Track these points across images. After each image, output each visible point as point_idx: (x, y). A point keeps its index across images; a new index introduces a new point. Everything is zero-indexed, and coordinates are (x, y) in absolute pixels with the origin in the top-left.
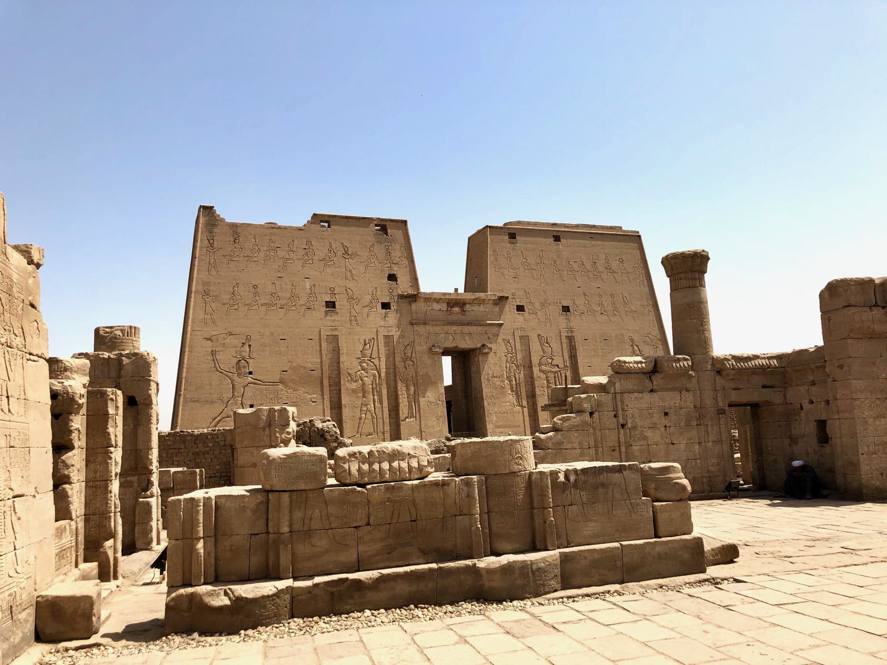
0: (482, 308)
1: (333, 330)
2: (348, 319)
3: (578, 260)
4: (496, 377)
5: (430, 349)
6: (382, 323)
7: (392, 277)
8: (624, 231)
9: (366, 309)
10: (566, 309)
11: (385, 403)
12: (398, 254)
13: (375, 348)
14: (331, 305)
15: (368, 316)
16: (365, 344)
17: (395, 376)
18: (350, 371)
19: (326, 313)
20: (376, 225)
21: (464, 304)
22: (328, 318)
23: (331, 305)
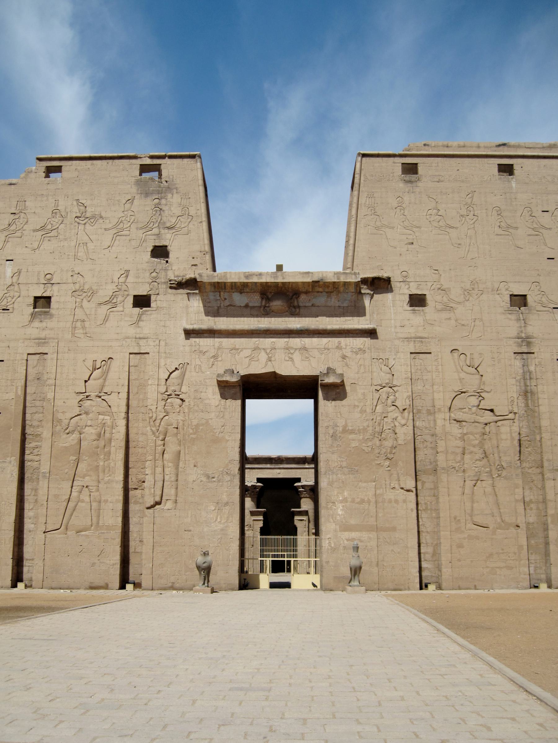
0: (334, 301)
1: (39, 344)
2: (69, 325)
4: (352, 432)
6: (132, 331)
7: (160, 252)
10: (519, 301)
12: (178, 212)
14: (42, 302)
15: (106, 319)
16: (95, 369)
18: (60, 416)
19: (33, 316)
20: (144, 169)
22: (36, 324)
23: (42, 302)
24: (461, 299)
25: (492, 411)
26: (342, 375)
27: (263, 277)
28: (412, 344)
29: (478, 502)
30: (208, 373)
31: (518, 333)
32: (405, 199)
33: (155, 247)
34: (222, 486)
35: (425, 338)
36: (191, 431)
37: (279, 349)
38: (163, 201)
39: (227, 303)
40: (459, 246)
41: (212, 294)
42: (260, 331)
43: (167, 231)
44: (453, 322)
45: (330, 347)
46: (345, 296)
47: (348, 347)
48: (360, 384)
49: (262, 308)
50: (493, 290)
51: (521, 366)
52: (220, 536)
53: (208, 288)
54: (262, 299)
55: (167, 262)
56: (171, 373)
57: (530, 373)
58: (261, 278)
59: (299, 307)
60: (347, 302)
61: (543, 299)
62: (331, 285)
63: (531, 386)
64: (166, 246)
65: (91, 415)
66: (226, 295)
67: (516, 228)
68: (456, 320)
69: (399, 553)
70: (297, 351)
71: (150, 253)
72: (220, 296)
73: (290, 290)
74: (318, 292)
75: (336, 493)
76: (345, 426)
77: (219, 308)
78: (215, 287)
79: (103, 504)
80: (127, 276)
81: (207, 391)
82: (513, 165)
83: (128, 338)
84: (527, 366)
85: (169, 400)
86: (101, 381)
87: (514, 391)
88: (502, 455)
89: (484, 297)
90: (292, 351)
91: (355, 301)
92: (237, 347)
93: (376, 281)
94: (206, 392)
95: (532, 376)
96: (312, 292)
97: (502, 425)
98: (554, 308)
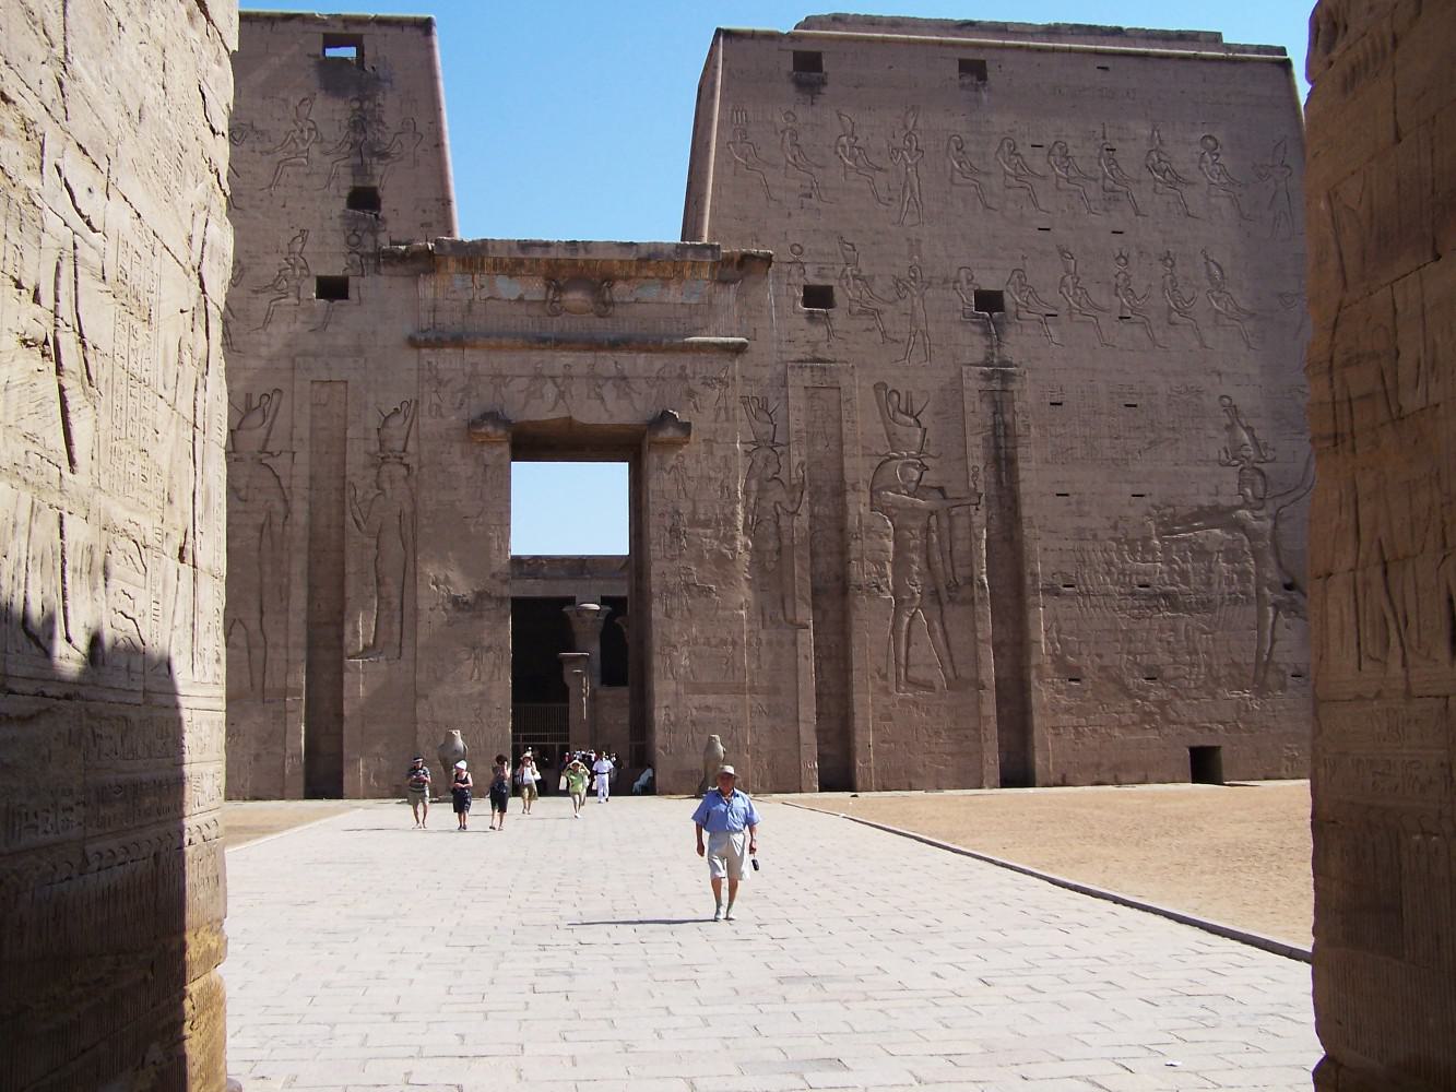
0: (673, 294)
3: (1048, 141)
4: (706, 524)
5: (473, 424)
7: (364, 199)
8: (1229, 47)
9: (263, 301)
10: (989, 301)
11: (299, 598)
13: (282, 422)
17: (344, 513)
20: (332, 41)
21: (610, 279)
24: (891, 295)
25: (941, 490)
27: (551, 249)
28: (807, 373)
29: (916, 644)
30: (453, 418)
31: (987, 358)
33: (355, 187)
34: (481, 617)
35: (829, 362)
36: (425, 522)
37: (577, 377)
38: (366, 104)
39: (485, 293)
40: (890, 202)
41: (458, 276)
43: (375, 159)
44: (877, 336)
45: (666, 375)
46: (695, 285)
47: (697, 377)
48: (720, 440)
49: (548, 304)
50: (946, 281)
51: (991, 414)
52: (477, 705)
53: (452, 265)
54: (548, 287)
55: (376, 216)
56: (386, 418)
57: (1006, 427)
59: (612, 303)
60: (695, 296)
61: (1031, 300)
63: (1006, 447)
64: (374, 190)
65: (242, 494)
67: (987, 174)
68: (883, 333)
69: (783, 731)
70: (611, 382)
71: (343, 203)
72: (473, 281)
73: (598, 273)
74: (647, 277)
75: (677, 628)
76: (694, 512)
77: (471, 301)
78: (464, 265)
79: (270, 651)
80: (304, 241)
81: (452, 450)
82: (984, 62)
83: (304, 354)
84: (1002, 414)
85: (385, 468)
86: (262, 432)
87: (977, 456)
88: (957, 564)
89: (930, 293)
90: (600, 382)
91: (710, 296)
92: (504, 372)
93: (746, 261)
94: (449, 453)
95: (1008, 432)
96: (636, 277)
97: (958, 514)
98: (1048, 315)
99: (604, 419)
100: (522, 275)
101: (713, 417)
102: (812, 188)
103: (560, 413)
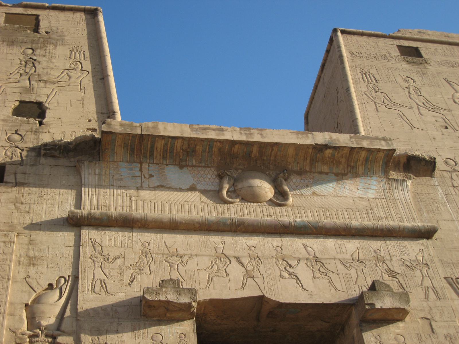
26: (405, 296)
32: (415, 79)
41: (124, 165)
42: (225, 224)
43: (42, 84)
47: (394, 259)
48: (437, 318)
54: (221, 177)
58: (223, 135)
62: (343, 160)
64: (40, 104)
66: (153, 169)
70: (303, 263)
72: (141, 170)
78: (132, 151)
92: (181, 252)
93: (412, 163)
96: (311, 172)
99: (303, 298)
100: (193, 166)
101: (422, 296)
102: (446, 122)
103: (250, 291)
